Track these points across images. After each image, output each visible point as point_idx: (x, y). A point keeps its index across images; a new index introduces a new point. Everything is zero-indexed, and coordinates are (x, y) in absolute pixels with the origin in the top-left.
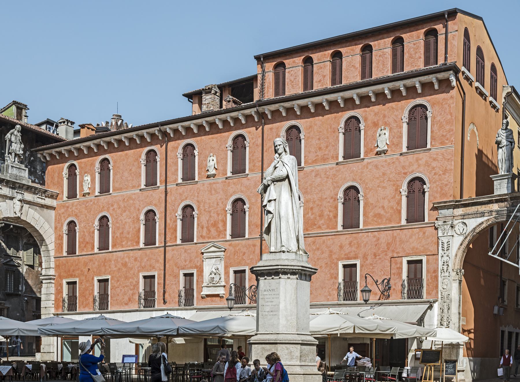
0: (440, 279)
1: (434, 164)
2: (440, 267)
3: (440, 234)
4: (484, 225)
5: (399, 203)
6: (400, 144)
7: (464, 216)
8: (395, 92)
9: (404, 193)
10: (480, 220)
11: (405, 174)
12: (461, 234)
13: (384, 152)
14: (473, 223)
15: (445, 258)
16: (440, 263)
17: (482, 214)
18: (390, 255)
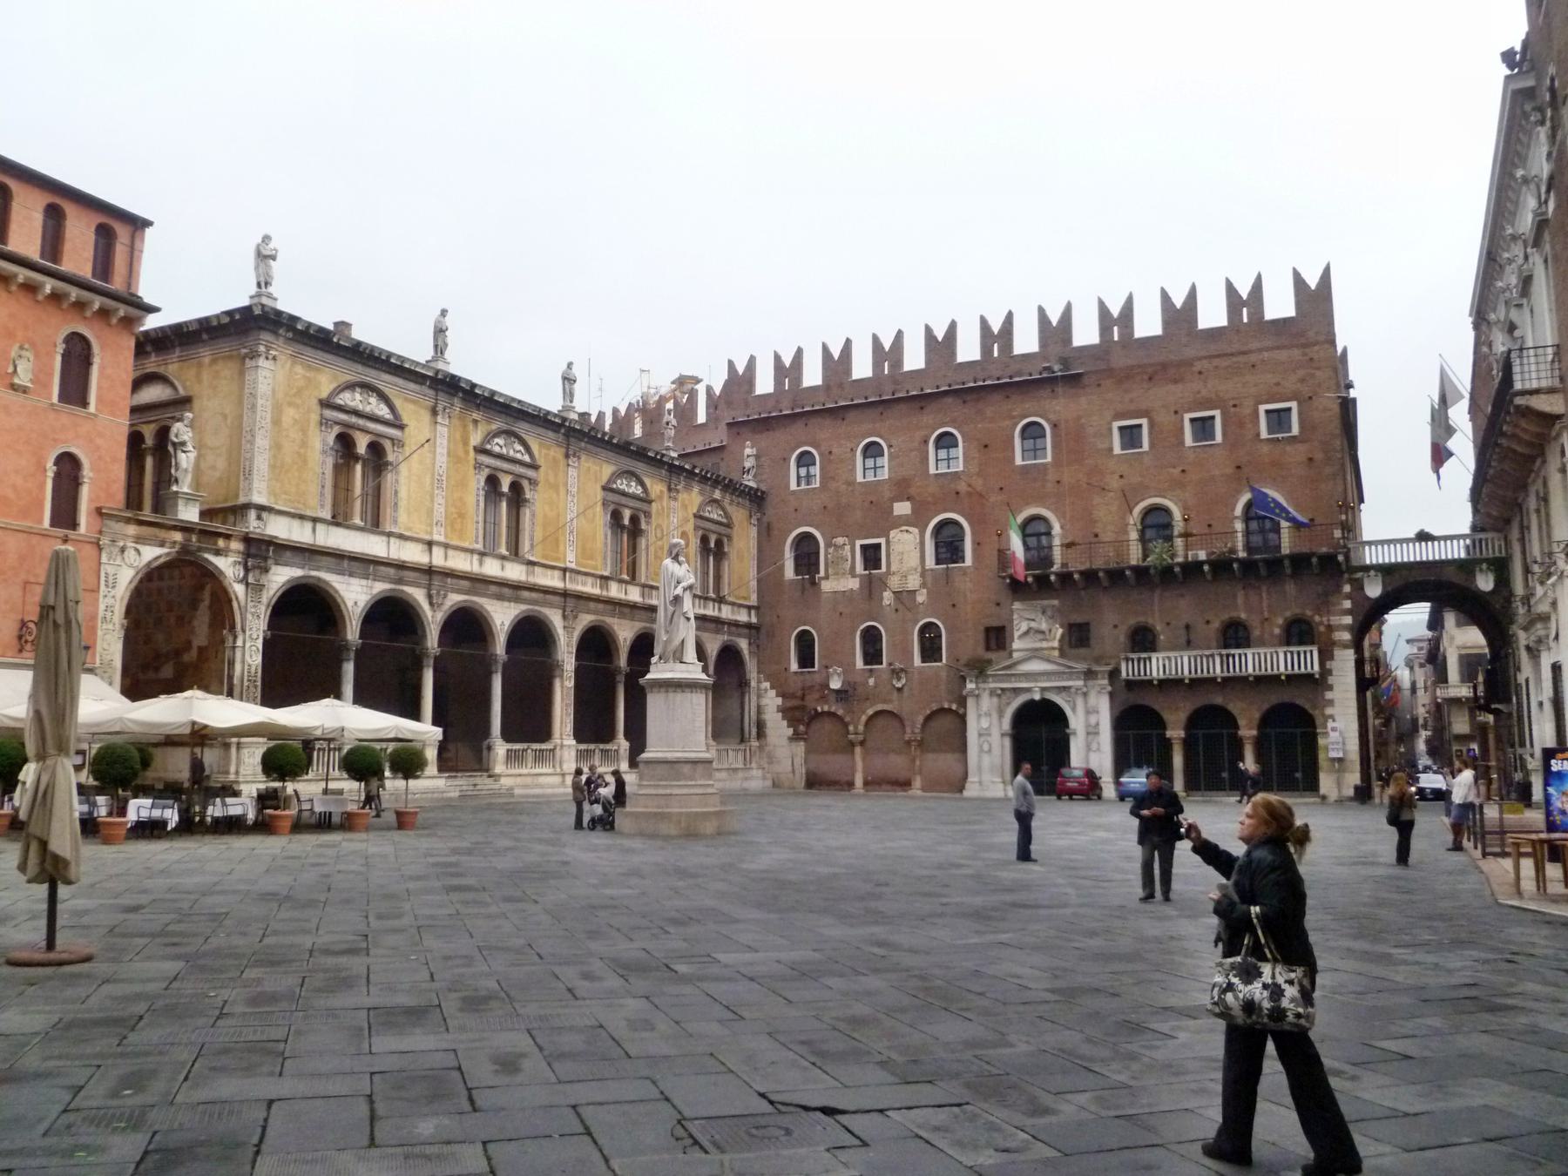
0: (100, 633)
1: (99, 441)
2: (101, 613)
3: (104, 559)
4: (162, 560)
5: (42, 486)
6: (47, 386)
7: (139, 540)
8: (56, 297)
9: (50, 474)
10: (158, 551)
11: (55, 440)
12: (131, 566)
13: (25, 390)
14: (150, 553)
15: (110, 601)
16: (102, 607)
17: (162, 545)
18: (23, 576)
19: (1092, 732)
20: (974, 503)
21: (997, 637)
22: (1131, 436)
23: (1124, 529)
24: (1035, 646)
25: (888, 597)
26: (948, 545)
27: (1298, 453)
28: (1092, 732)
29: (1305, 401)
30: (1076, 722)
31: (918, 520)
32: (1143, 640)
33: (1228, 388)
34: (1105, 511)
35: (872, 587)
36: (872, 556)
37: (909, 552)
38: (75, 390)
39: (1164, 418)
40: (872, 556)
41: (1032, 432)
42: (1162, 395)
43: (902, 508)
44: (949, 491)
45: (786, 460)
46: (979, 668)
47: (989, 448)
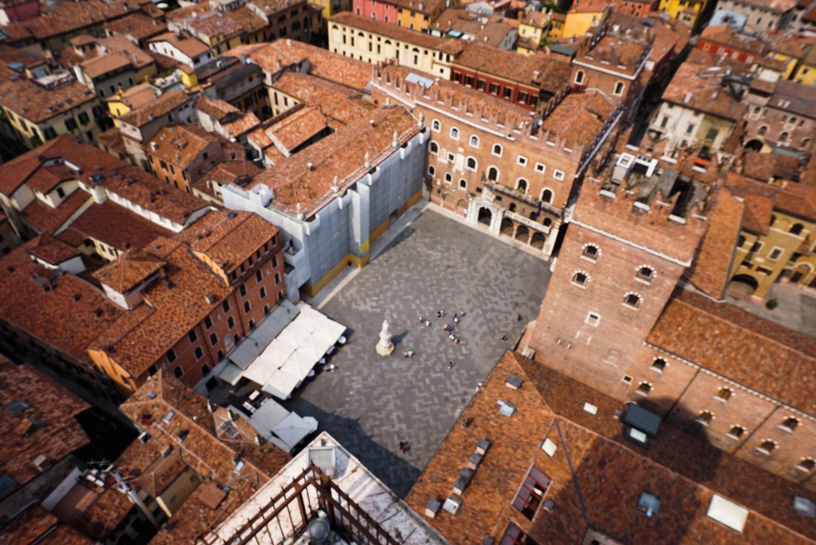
19: (496, 219)
20: (480, 158)
21: (479, 190)
22: (522, 161)
23: (514, 181)
24: (486, 199)
25: (454, 170)
26: (471, 163)
27: (561, 185)
28: (496, 219)
29: (567, 174)
30: (494, 215)
31: (465, 153)
32: (512, 208)
33: (549, 161)
34: (511, 175)
35: (450, 165)
36: (451, 157)
37: (460, 162)
38: (275, 265)
39: (531, 160)
40: (451, 157)
41: (498, 149)
42: (533, 155)
43: (461, 150)
44: (473, 152)
45: (431, 120)
46: (473, 195)
47: (485, 146)
